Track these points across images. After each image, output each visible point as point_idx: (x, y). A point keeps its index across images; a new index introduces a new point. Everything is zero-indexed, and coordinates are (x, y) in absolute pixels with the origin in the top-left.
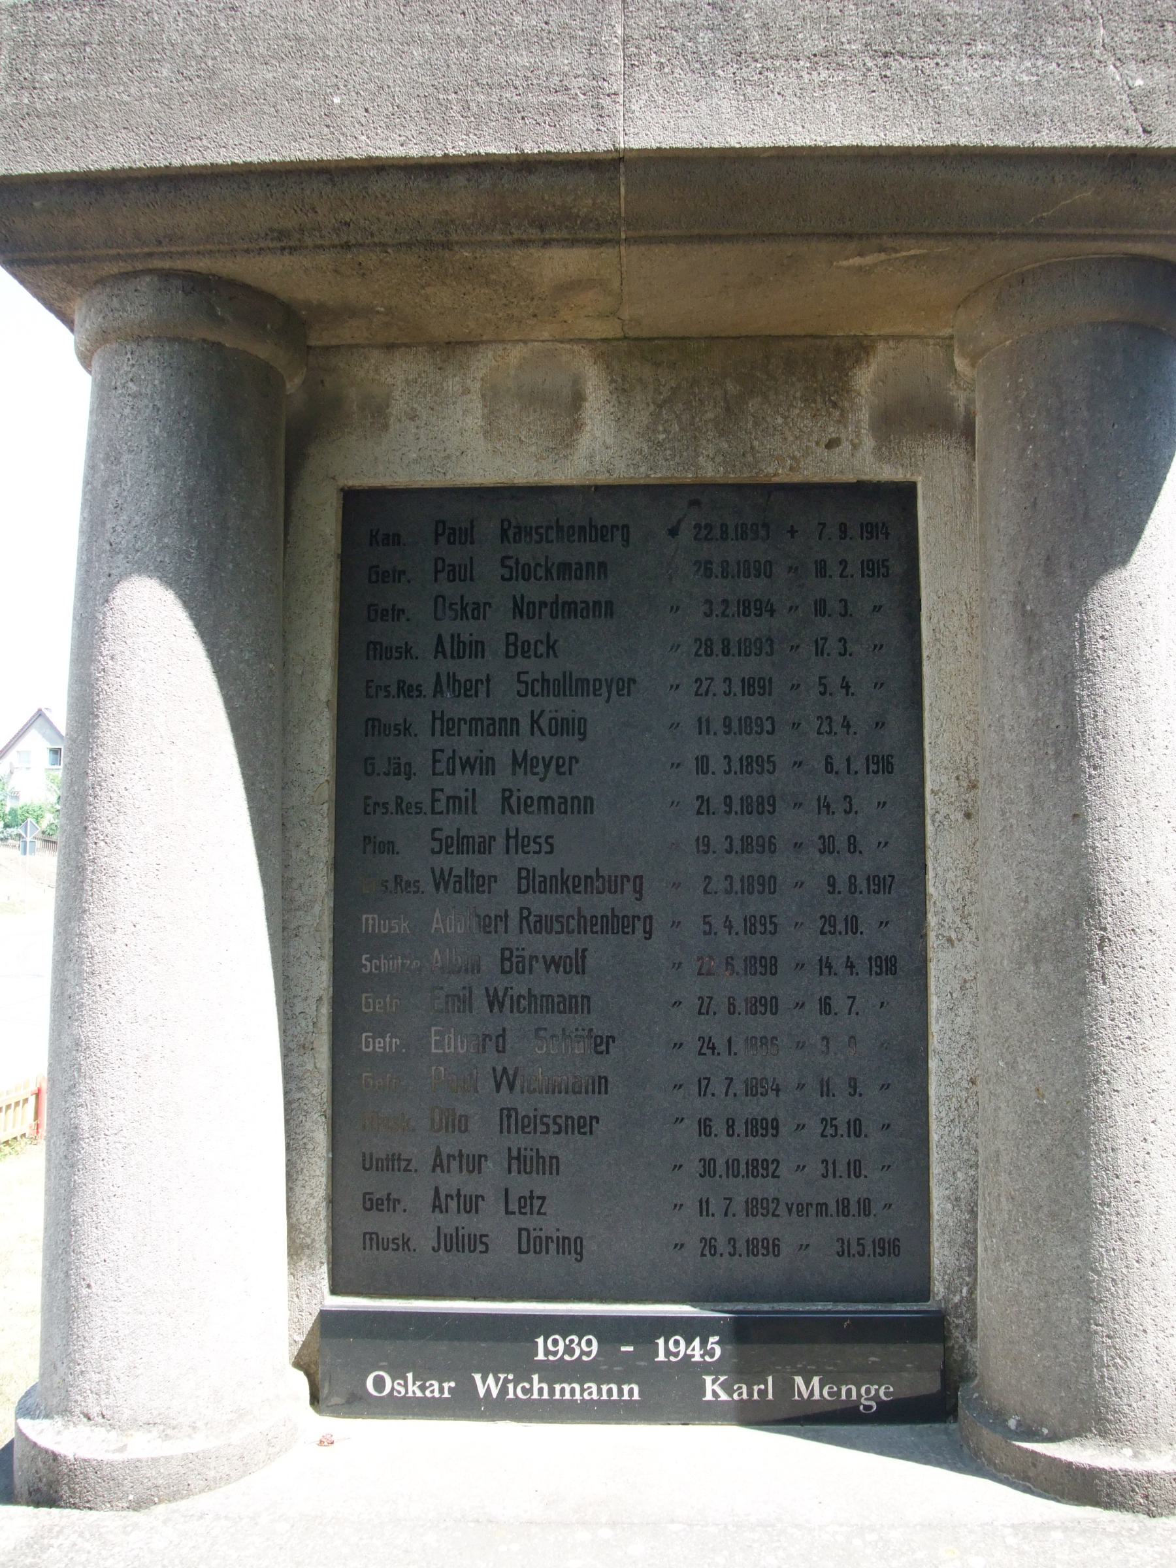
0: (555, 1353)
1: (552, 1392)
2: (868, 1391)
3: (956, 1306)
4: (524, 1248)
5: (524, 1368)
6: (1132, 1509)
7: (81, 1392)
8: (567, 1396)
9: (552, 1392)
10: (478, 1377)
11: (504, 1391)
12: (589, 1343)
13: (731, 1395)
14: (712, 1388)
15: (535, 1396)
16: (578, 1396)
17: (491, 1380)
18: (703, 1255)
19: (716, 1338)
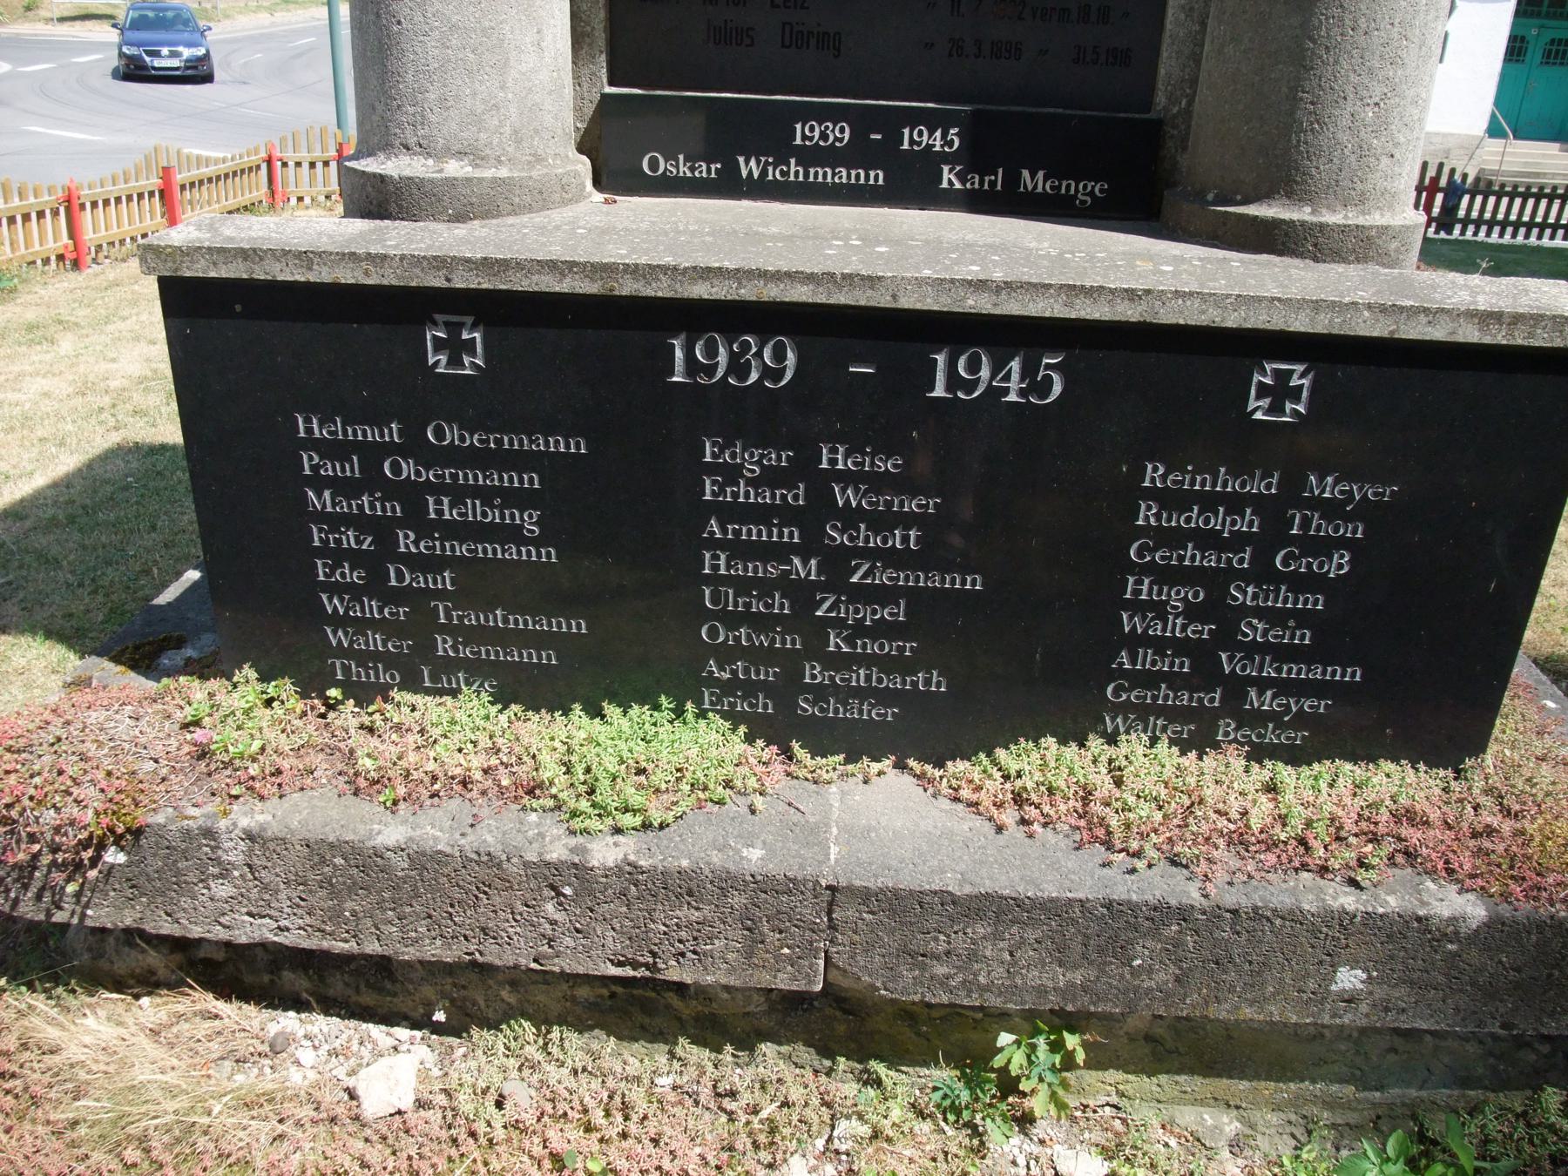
0: (811, 139)
1: (806, 175)
2: (1085, 187)
3: (1175, 117)
4: (787, 43)
5: (782, 149)
6: (1301, 256)
7: (399, 125)
8: (820, 179)
9: (806, 175)
10: (741, 160)
11: (764, 173)
12: (842, 130)
13: (964, 184)
14: (949, 177)
15: (792, 178)
16: (829, 179)
17: (753, 163)
18: (950, 55)
19: (956, 130)
